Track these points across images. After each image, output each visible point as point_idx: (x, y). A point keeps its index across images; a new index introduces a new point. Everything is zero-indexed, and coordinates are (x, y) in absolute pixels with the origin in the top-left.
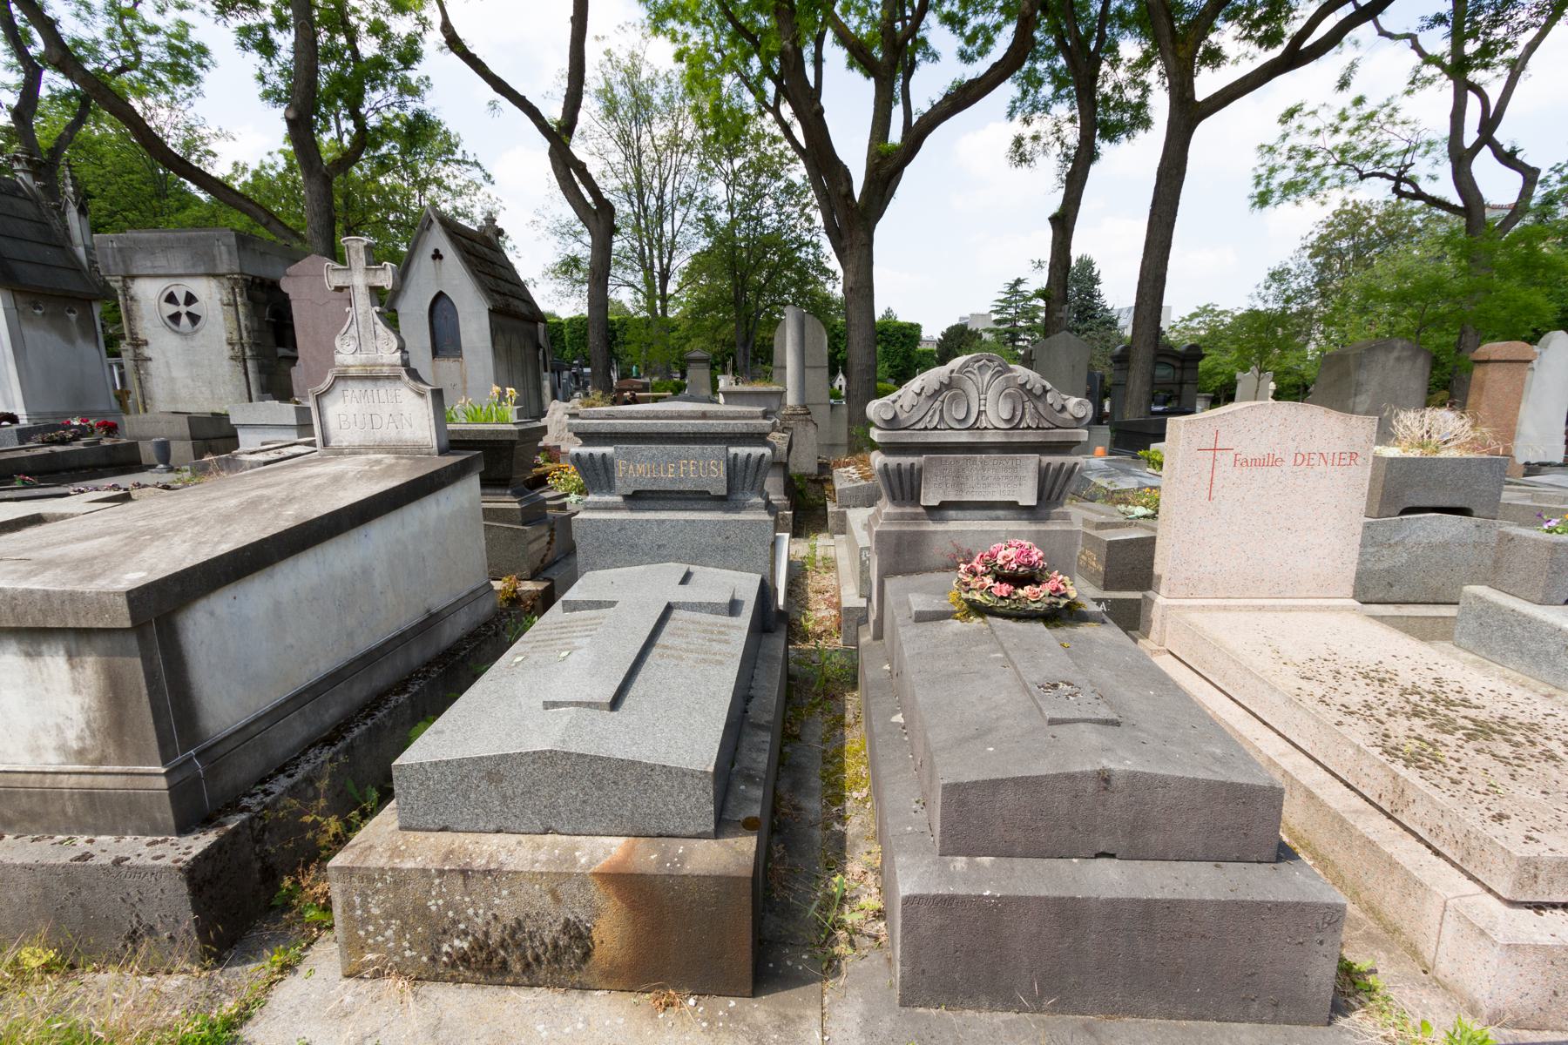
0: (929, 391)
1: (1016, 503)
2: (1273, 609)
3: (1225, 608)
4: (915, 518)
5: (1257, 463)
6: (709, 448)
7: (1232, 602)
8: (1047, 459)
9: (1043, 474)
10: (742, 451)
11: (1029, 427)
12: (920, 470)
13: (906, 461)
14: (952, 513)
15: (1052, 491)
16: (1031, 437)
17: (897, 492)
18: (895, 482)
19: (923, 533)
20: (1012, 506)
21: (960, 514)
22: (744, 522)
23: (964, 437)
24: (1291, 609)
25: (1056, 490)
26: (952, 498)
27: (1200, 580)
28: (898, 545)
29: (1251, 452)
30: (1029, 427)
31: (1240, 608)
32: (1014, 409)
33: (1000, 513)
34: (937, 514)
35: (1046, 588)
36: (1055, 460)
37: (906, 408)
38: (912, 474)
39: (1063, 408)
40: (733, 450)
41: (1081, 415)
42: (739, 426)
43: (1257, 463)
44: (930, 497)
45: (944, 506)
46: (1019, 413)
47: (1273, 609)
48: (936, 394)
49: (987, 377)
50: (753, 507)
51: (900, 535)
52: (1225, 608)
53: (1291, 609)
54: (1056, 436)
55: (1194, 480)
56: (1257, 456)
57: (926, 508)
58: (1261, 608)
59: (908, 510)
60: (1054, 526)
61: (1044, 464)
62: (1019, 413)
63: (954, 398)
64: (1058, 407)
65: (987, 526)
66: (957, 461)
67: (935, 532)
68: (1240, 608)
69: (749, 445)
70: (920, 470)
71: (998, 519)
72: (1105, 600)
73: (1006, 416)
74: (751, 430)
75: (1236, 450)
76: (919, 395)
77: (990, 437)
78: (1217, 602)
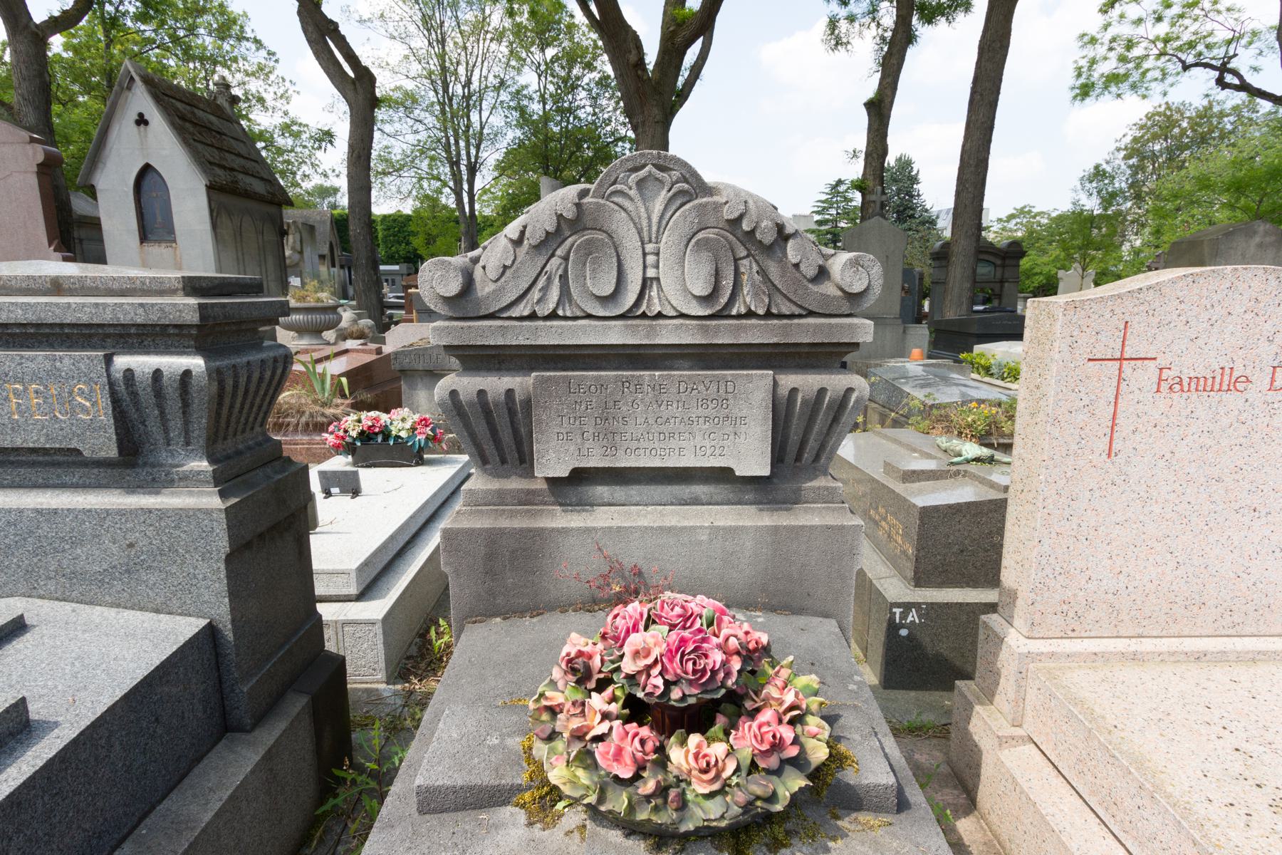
0: (533, 237)
1: (729, 471)
2: (1222, 658)
3: (1136, 658)
4: (528, 499)
5: (1200, 385)
6: (67, 359)
7: (1147, 645)
8: (789, 380)
9: (781, 412)
10: (142, 363)
11: (750, 314)
12: (527, 404)
13: (497, 384)
14: (602, 491)
15: (800, 447)
16: (756, 334)
17: (489, 448)
18: (481, 428)
19: (542, 530)
20: (723, 475)
21: (619, 492)
22: (162, 514)
23: (616, 335)
24: (1254, 658)
25: (812, 444)
26: (592, 463)
27: (1089, 606)
28: (491, 556)
29: (1189, 365)
30: (750, 314)
31: (1163, 658)
32: (717, 275)
33: (700, 490)
34: (572, 493)
35: (747, 739)
36: (806, 382)
37: (492, 274)
38: (512, 412)
39: (823, 274)
40: (122, 362)
41: (857, 288)
42: (128, 309)
43: (1200, 385)
44: (554, 460)
45: (580, 476)
46: (727, 283)
47: (1222, 658)
48: (550, 241)
49: (658, 206)
50: (189, 480)
51: (493, 537)
52: (1135, 657)
53: (1254, 658)
54: (806, 331)
55: (1081, 417)
56: (1200, 372)
57: (548, 479)
58: (1199, 657)
59: (515, 484)
60: (809, 517)
61: (783, 392)
62: (727, 283)
63: (589, 249)
64: (810, 271)
65: (674, 517)
66: (602, 386)
67: (565, 531)
68: (1163, 658)
69: (167, 351)
70: (527, 404)
71: (696, 502)
72: (917, 606)
73: (701, 289)
74: (154, 318)
75: (1162, 362)
76: (518, 243)
77: (668, 335)
78: (1120, 645)
